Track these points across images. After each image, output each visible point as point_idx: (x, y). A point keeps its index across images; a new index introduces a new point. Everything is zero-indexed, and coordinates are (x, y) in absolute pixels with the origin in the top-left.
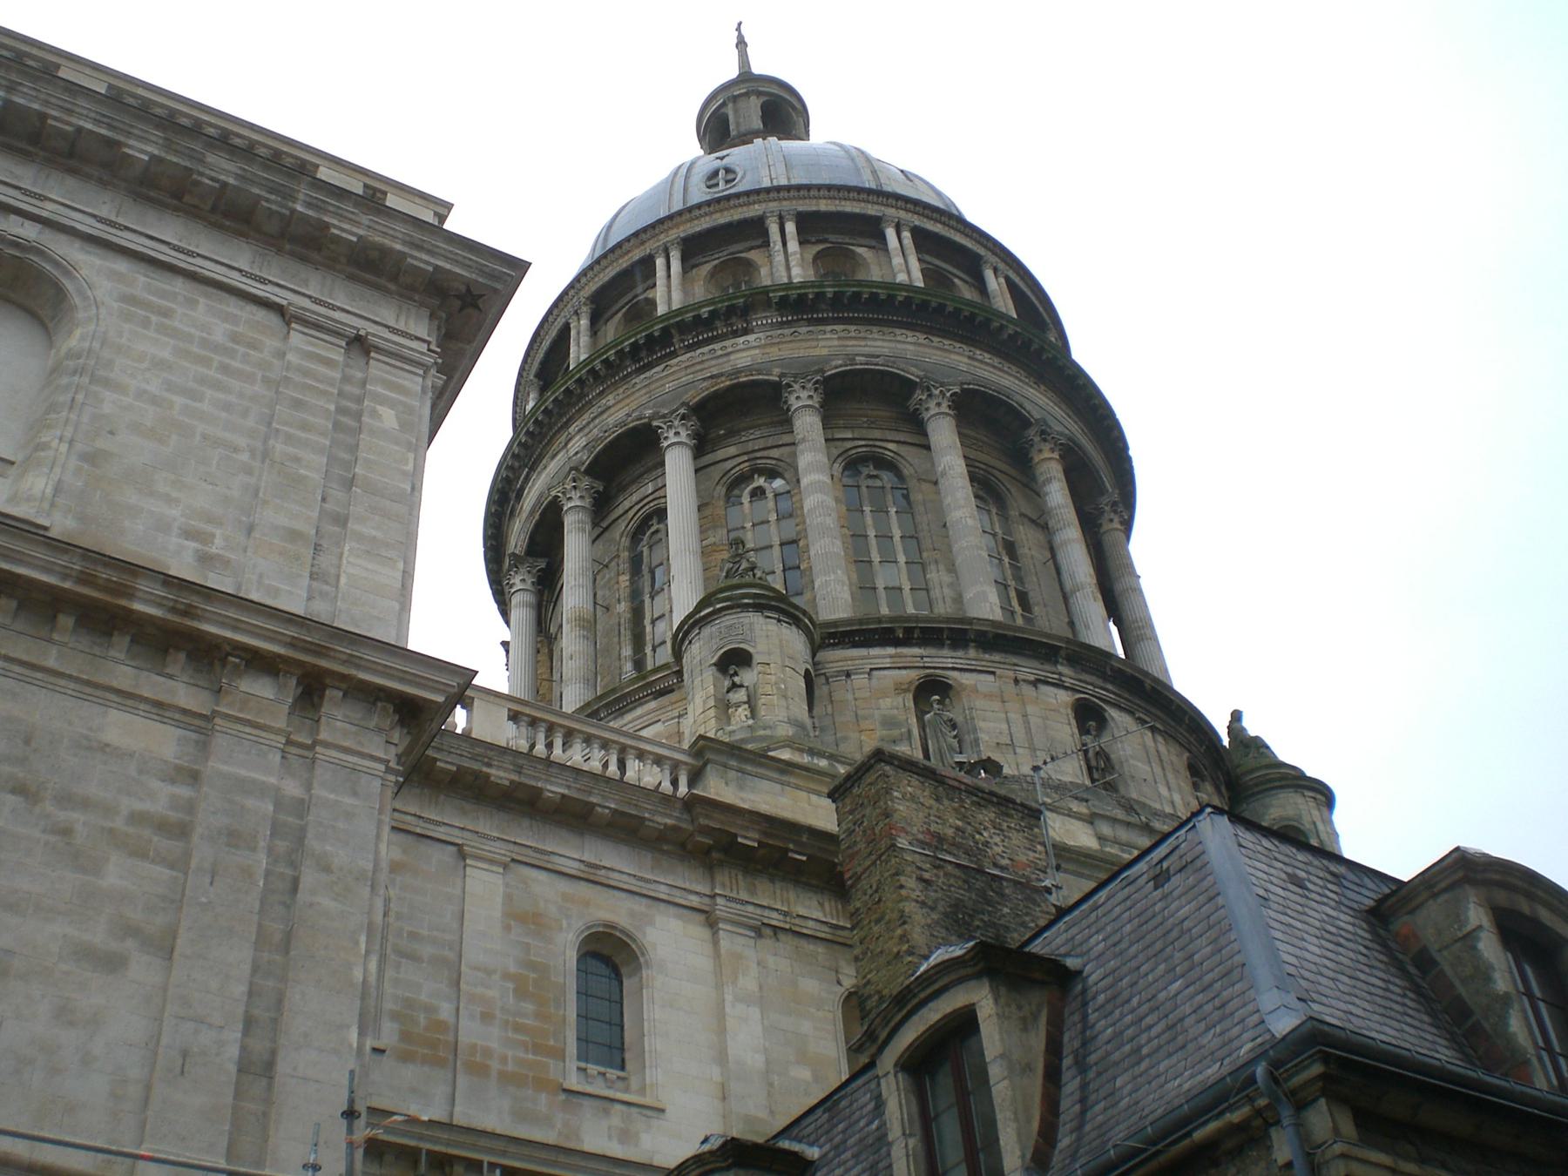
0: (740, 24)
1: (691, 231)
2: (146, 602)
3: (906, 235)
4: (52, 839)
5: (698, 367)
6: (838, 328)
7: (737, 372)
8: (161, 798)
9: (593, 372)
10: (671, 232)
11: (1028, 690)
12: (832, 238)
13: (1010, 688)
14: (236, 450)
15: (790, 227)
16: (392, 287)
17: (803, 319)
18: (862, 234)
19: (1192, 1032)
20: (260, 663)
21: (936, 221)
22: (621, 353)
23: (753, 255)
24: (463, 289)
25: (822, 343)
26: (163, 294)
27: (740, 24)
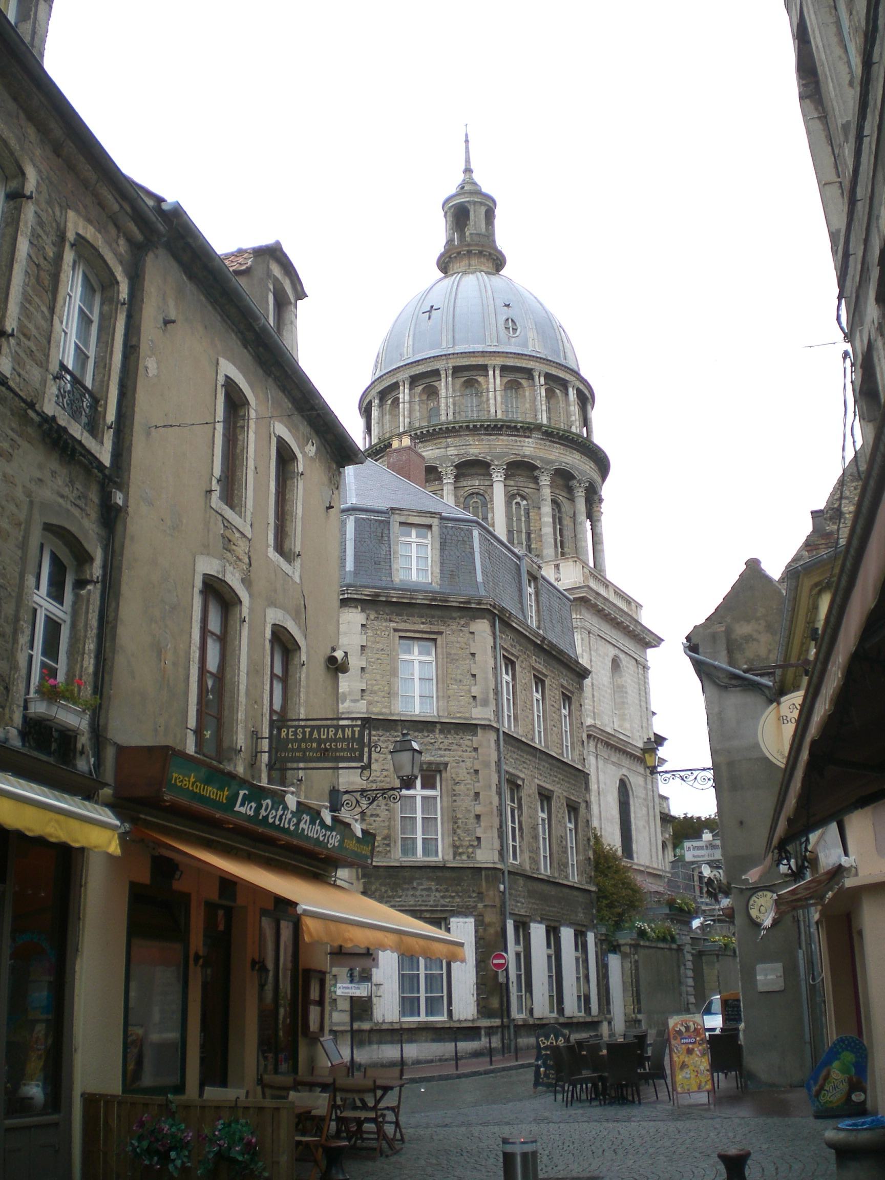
3: (575, 392)
5: (511, 447)
6: (558, 446)
7: (525, 456)
9: (468, 427)
18: (561, 385)
22: (482, 426)
25: (553, 453)
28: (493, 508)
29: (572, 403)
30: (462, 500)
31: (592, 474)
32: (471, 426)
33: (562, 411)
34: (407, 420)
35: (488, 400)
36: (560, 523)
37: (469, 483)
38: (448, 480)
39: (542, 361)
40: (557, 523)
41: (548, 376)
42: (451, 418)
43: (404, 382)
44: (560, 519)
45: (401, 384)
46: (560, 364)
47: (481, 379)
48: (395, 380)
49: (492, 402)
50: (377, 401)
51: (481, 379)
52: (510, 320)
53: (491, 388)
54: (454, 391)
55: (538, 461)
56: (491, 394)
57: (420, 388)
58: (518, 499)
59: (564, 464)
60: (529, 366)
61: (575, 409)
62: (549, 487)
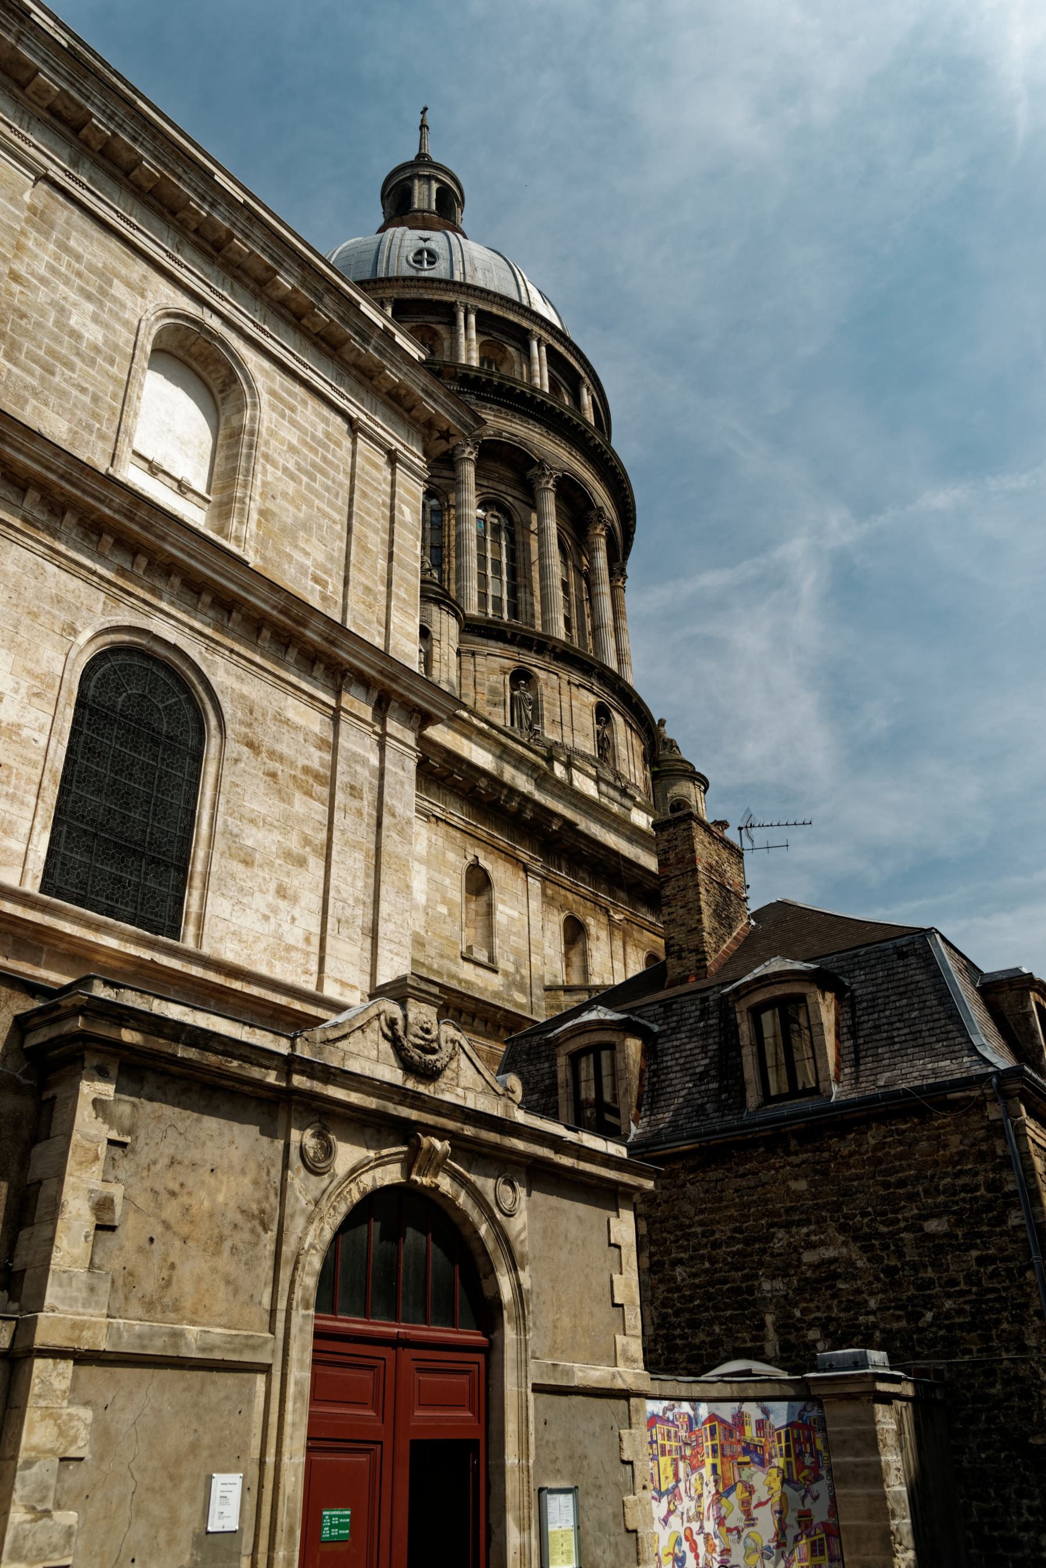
0: (426, 109)
1: (402, 296)
2: (314, 632)
3: (543, 349)
4: (268, 779)
6: (495, 407)
8: (317, 759)
10: (387, 291)
11: (574, 688)
12: (495, 334)
13: (565, 686)
14: (334, 522)
15: (472, 318)
16: (406, 415)
18: (514, 338)
19: (927, 1040)
20: (364, 682)
21: (561, 343)
23: (440, 328)
24: (445, 428)
26: (290, 393)
27: (426, 109)
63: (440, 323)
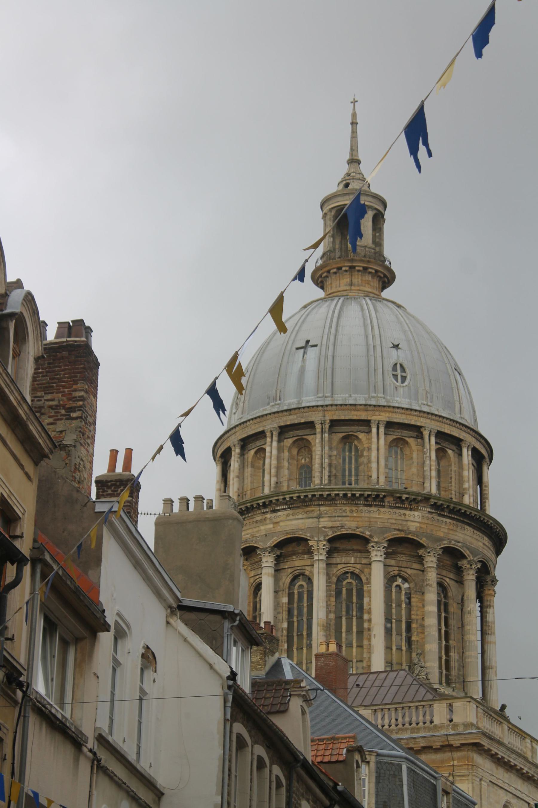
3: (470, 453)
17: (437, 513)
18: (453, 443)
22: (361, 495)
23: (411, 441)
25: (442, 530)
28: (369, 592)
29: (465, 467)
30: (334, 579)
31: (485, 552)
32: (349, 495)
33: (453, 476)
34: (274, 480)
35: (369, 461)
36: (446, 611)
37: (343, 560)
38: (320, 556)
39: (434, 417)
40: (442, 610)
41: (440, 435)
42: (326, 481)
43: (272, 432)
44: (446, 605)
45: (268, 434)
46: (454, 421)
47: (361, 436)
48: (261, 429)
49: (374, 465)
50: (238, 450)
51: (361, 436)
52: (398, 366)
53: (374, 446)
54: (331, 448)
55: (424, 539)
56: (374, 454)
57: (290, 441)
58: (400, 580)
59: (453, 542)
60: (419, 424)
61: (469, 474)
62: (434, 570)
63: (411, 437)
